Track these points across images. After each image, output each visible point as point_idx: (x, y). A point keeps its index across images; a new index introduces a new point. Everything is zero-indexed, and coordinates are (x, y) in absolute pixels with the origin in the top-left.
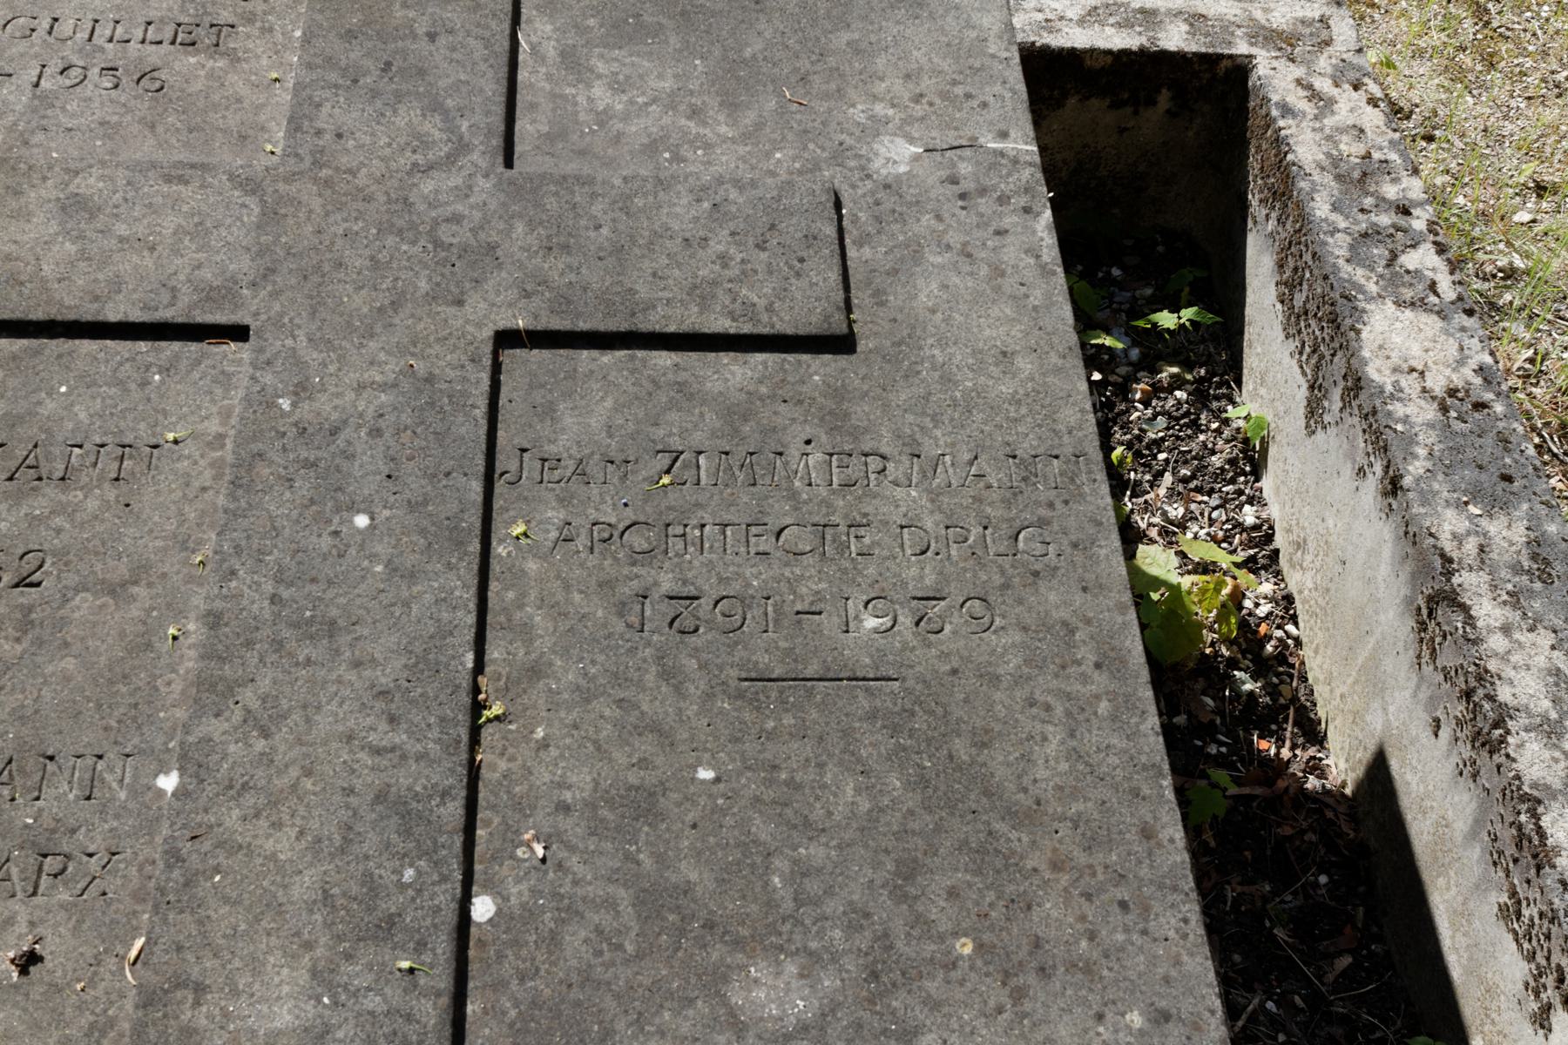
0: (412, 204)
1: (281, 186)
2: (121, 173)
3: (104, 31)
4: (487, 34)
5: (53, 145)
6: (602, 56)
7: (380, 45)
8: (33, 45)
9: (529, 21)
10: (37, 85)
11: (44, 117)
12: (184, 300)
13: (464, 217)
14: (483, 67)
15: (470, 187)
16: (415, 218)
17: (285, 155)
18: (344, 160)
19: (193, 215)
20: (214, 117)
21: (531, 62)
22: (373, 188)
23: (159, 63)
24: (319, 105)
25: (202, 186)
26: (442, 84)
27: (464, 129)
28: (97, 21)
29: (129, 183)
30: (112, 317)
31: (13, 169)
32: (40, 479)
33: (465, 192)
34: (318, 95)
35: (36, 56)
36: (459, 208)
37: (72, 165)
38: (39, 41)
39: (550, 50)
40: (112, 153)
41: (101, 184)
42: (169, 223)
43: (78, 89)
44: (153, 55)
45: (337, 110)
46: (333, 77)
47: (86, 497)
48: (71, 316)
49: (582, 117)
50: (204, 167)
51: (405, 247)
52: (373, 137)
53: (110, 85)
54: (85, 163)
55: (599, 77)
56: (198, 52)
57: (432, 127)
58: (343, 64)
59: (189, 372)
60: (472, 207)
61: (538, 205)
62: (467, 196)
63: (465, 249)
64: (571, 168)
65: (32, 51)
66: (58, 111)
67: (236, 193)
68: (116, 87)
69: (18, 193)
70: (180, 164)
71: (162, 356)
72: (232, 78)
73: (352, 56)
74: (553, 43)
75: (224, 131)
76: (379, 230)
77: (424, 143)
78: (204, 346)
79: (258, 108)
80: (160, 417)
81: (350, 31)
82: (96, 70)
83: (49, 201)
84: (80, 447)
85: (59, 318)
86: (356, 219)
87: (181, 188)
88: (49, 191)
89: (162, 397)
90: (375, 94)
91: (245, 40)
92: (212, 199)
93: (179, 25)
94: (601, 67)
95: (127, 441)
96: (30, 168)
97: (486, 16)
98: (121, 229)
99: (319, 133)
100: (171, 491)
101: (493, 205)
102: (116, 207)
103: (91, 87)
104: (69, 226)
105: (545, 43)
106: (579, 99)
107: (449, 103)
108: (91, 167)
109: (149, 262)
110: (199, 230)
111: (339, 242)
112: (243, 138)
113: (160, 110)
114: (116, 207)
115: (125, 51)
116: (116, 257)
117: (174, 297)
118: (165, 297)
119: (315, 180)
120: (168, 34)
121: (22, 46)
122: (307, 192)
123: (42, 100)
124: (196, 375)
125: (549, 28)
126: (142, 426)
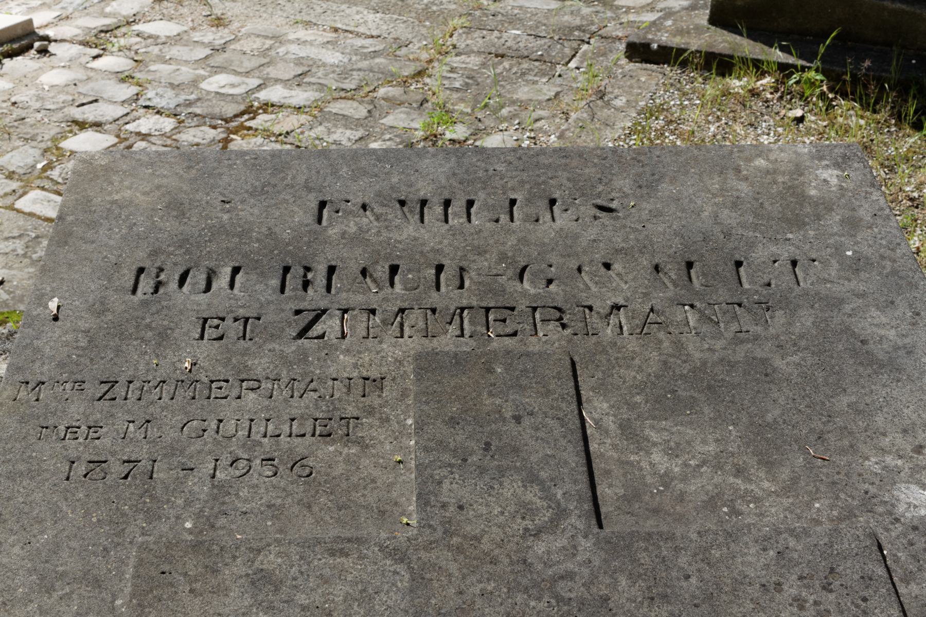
0: (531, 565)
1: (423, 554)
2: (293, 549)
4: (561, 415)
5: (234, 527)
6: (652, 427)
7: (478, 429)
8: (206, 444)
9: (589, 401)
10: (213, 476)
11: (224, 503)
13: (575, 573)
14: (563, 442)
15: (575, 547)
16: (535, 576)
17: (420, 527)
18: (469, 528)
19: (357, 584)
21: (597, 435)
22: (497, 552)
23: (306, 452)
24: (440, 483)
25: (359, 558)
26: (534, 458)
27: (559, 496)
28: (252, 420)
29: (302, 558)
31: (208, 550)
33: (572, 551)
34: (438, 473)
36: (570, 566)
37: (255, 545)
38: (210, 440)
39: (610, 423)
40: (281, 531)
41: (279, 560)
42: (339, 591)
43: (246, 478)
45: (455, 486)
46: (446, 457)
49: (649, 480)
50: (359, 541)
51: (533, 603)
52: (493, 508)
54: (264, 542)
55: (655, 444)
56: (334, 442)
57: (532, 495)
58: (452, 445)
60: (580, 565)
61: (634, 561)
62: (574, 555)
63: (582, 603)
64: (649, 525)
67: (388, 562)
68: (275, 474)
73: (458, 438)
74: (611, 418)
76: (509, 589)
77: (526, 510)
79: (390, 486)
81: (452, 418)
82: (258, 461)
83: (241, 577)
86: (488, 580)
87: (343, 559)
88: (239, 568)
90: (482, 470)
91: (369, 429)
92: (369, 569)
93: (316, 420)
94: (654, 436)
97: (557, 399)
98: (302, 599)
99: (444, 506)
101: (597, 562)
102: (295, 579)
103: (256, 476)
104: (260, 598)
105: (605, 418)
106: (643, 464)
107: (543, 475)
108: (269, 545)
111: (479, 602)
112: (382, 513)
113: (313, 492)
114: (295, 579)
119: (449, 547)
120: (309, 429)
121: (198, 445)
122: (443, 557)
123: (220, 490)
125: (605, 405)
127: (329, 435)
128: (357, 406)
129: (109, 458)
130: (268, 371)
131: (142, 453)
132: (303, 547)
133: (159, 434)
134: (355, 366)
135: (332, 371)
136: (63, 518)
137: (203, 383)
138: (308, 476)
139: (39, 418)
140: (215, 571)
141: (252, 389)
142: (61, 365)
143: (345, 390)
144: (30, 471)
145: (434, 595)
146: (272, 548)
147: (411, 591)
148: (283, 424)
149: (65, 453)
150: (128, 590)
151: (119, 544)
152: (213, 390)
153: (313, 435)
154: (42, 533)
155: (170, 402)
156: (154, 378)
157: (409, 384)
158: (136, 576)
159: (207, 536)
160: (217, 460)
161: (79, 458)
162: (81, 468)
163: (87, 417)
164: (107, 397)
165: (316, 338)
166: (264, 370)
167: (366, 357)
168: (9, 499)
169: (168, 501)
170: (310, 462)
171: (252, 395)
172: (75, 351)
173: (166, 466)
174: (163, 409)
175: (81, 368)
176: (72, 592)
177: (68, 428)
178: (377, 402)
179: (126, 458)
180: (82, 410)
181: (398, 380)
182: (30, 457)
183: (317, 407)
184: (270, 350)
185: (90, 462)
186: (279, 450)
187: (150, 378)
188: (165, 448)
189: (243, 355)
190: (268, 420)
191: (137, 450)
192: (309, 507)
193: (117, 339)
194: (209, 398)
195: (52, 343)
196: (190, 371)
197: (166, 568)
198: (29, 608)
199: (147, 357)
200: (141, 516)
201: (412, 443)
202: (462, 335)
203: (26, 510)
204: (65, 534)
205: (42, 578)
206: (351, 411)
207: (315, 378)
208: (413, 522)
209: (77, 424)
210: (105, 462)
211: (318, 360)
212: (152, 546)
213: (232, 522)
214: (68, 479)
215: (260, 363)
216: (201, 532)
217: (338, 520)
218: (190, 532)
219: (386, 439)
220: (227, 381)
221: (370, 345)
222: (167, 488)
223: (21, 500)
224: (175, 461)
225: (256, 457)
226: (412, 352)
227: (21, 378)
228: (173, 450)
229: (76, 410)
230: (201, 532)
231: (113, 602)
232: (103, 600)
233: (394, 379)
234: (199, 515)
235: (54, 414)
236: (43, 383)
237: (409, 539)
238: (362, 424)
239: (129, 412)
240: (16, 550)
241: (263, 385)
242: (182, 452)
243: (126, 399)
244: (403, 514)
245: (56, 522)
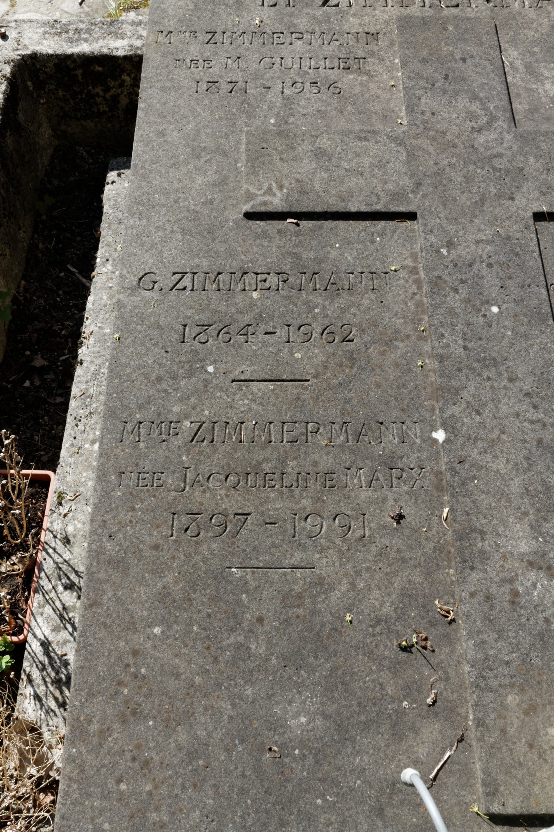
0: (476, 148)
1: (412, 141)
2: (336, 136)
3: (306, 63)
4: (490, 58)
6: (545, 67)
7: (440, 66)
8: (275, 72)
9: (506, 50)
10: (283, 93)
11: (291, 109)
12: (384, 201)
13: (503, 154)
14: (493, 75)
15: (502, 139)
16: (479, 155)
18: (438, 126)
20: (369, 106)
21: (511, 72)
22: (456, 140)
23: (336, 79)
24: (419, 99)
26: (475, 85)
27: (491, 108)
28: (301, 58)
29: (342, 142)
32: (338, 290)
33: (500, 141)
34: (418, 93)
36: (500, 150)
37: (314, 133)
38: (278, 70)
39: (519, 64)
41: (329, 142)
42: (366, 161)
43: (302, 93)
45: (428, 101)
46: (422, 83)
47: (362, 298)
48: (334, 209)
49: (544, 100)
50: (374, 132)
51: (479, 171)
52: (453, 114)
53: (316, 91)
54: (319, 132)
55: (547, 78)
56: (352, 73)
57: (475, 107)
58: (425, 76)
59: (392, 236)
60: (505, 149)
61: (537, 147)
62: (502, 144)
63: (508, 171)
64: (544, 127)
65: (276, 75)
67: (393, 145)
69: (293, 148)
70: (362, 131)
72: (372, 86)
73: (428, 71)
74: (520, 61)
76: (465, 162)
77: (472, 117)
78: (395, 223)
79: (389, 100)
80: (385, 259)
81: (424, 59)
82: (308, 84)
83: (308, 152)
84: (353, 273)
85: (329, 210)
86: (452, 157)
87: (366, 143)
89: (383, 249)
90: (444, 92)
91: (372, 65)
92: (382, 149)
93: (340, 59)
94: (546, 73)
95: (373, 271)
97: (487, 48)
98: (345, 165)
99: (423, 113)
100: (399, 295)
101: (515, 148)
102: (340, 154)
103: (308, 93)
104: (321, 164)
105: (516, 61)
106: (540, 90)
107: (481, 95)
109: (362, 181)
110: (382, 164)
111: (448, 170)
112: (385, 117)
113: (343, 103)
114: (340, 154)
116: (347, 179)
117: (378, 199)
118: (375, 199)
119: (428, 137)
120: (336, 65)
121: (270, 73)
122: (424, 143)
123: (288, 101)
124: (396, 238)
125: (516, 53)
126: (378, 263)
127: (349, 68)
128: (363, 50)
129: (219, 80)
130: (307, 27)
131: (239, 77)
132: (342, 135)
133: (246, 66)
134: (360, 25)
135: (346, 27)
136: (198, 115)
137: (268, 34)
138: (339, 93)
139: (173, 54)
140: (293, 148)
141: (299, 39)
142: (180, 21)
143: (355, 40)
144: (174, 87)
145: (421, 165)
146: (324, 135)
147: (408, 162)
148: (321, 61)
149: (193, 76)
150: (244, 157)
151: (233, 131)
152: (275, 39)
153: (339, 68)
154: (188, 123)
155: (250, 46)
156: (238, 30)
157: (394, 37)
158: (248, 150)
159: (285, 127)
160: (283, 83)
161: (202, 80)
162: (205, 86)
163: (202, 54)
164: (211, 42)
165: (334, 6)
166: (305, 26)
167: (366, 19)
168: (165, 103)
169: (258, 107)
170: (339, 85)
171: (299, 43)
172: (187, 12)
173: (254, 86)
174: (247, 50)
175: (193, 23)
176: (211, 159)
177: (191, 61)
178: (376, 48)
179: (229, 80)
180: (198, 49)
181: (387, 35)
182: (172, 78)
183: (340, 51)
184: (306, 14)
185: (208, 82)
186: (320, 77)
187: (236, 30)
188: (251, 74)
189: (291, 16)
190: (311, 58)
191: (235, 75)
192: (342, 112)
193: (211, 5)
194: (273, 44)
195: (172, 7)
196: (259, 26)
197: (265, 145)
198: (189, 167)
199: (232, 17)
200: (244, 115)
201: (400, 74)
202: (424, 6)
203: (176, 110)
204: (202, 125)
205: (193, 150)
206: (360, 54)
207: (336, 32)
208: (405, 122)
209: (197, 58)
210: (217, 82)
211: (337, 20)
212: (254, 133)
213: (298, 120)
214: (197, 92)
215: (301, 22)
216: (280, 125)
217: (360, 120)
218: (274, 125)
219: (383, 71)
220: (283, 33)
221: (368, 11)
222: (256, 99)
223: (172, 104)
224: (259, 82)
225: (306, 81)
226: (395, 17)
227: (158, 29)
228: (256, 76)
229: (195, 50)
230: (280, 125)
231: (236, 164)
232: (230, 163)
233: (385, 34)
234: (277, 116)
235: (182, 52)
236: (172, 32)
237: (404, 132)
238: (368, 62)
239: (226, 51)
240: (175, 133)
241: (305, 36)
242: (262, 77)
243: (223, 43)
244: (398, 117)
245: (195, 118)
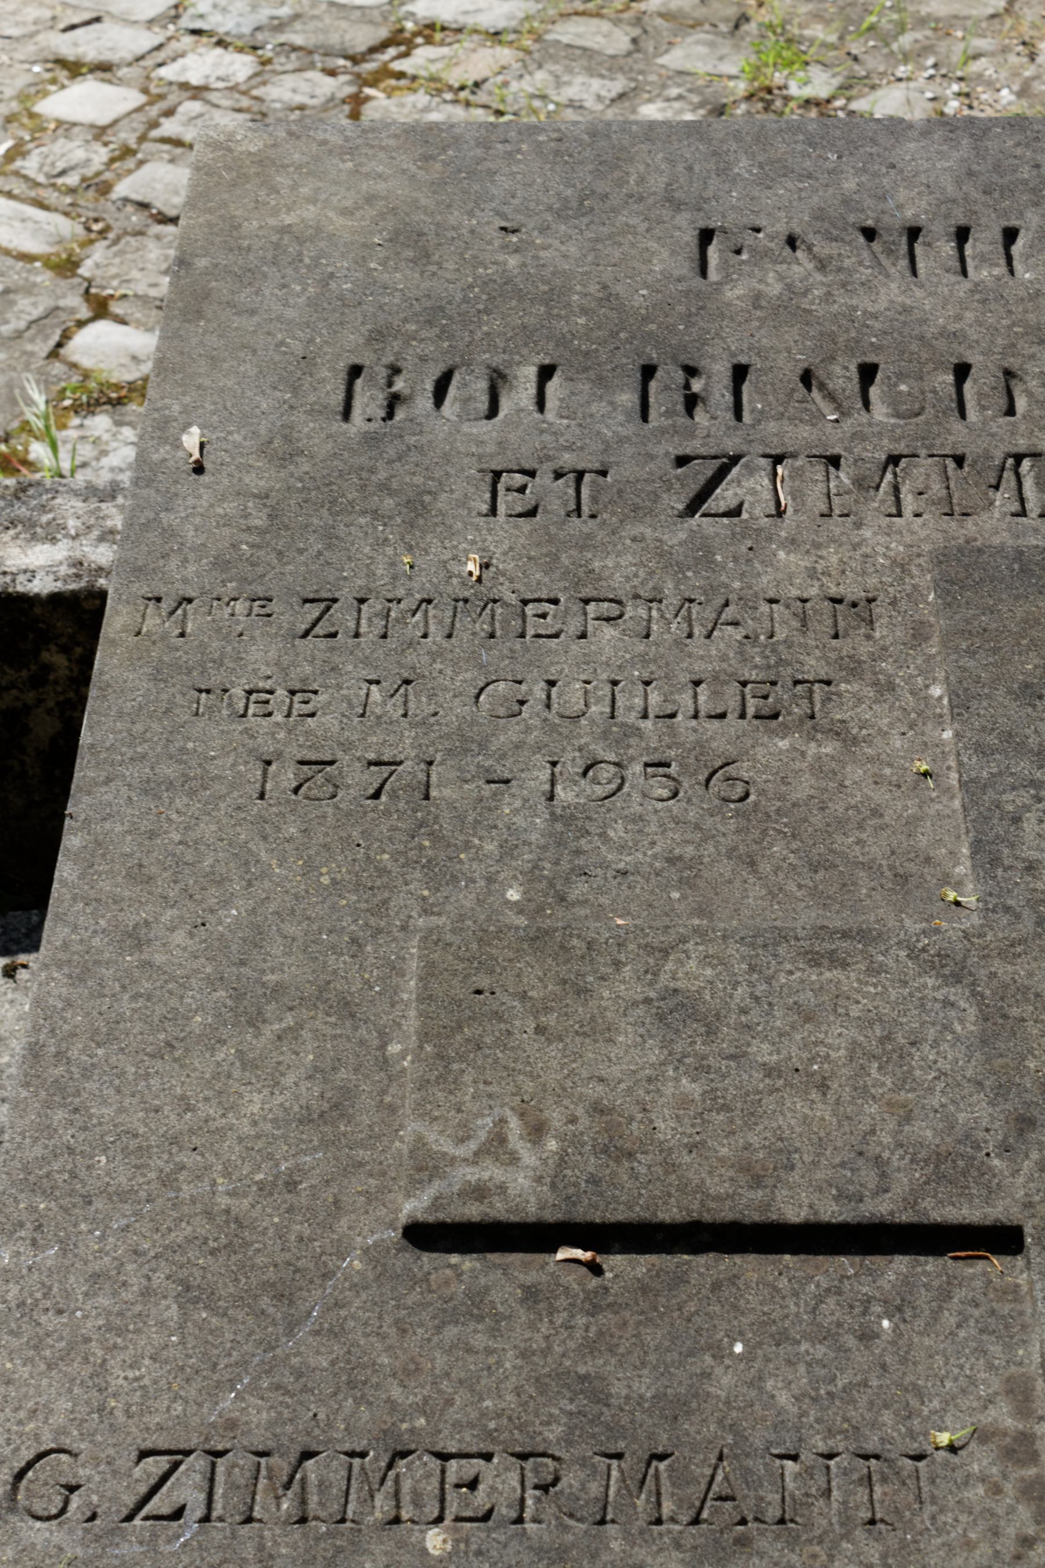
2: (733, 949)
3: (630, 700)
5: (604, 900)
8: (528, 730)
10: (551, 797)
11: (578, 852)
12: (901, 1183)
17: (986, 911)
19: (871, 1024)
20: (844, 842)
23: (732, 751)
24: (1017, 820)
25: (871, 971)
28: (615, 683)
29: (752, 969)
30: (794, 1213)
31: (562, 947)
32: (743, 1522)
35: (538, 748)
37: (656, 939)
38: (535, 722)
40: (700, 912)
41: (709, 972)
42: (838, 1037)
43: (618, 801)
44: (722, 737)
46: (1024, 767)
47: (831, 1558)
48: (726, 1214)
50: (864, 935)
53: (665, 793)
54: (672, 937)
56: (785, 731)
59: (936, 1315)
65: (531, 738)
66: (597, 842)
67: (930, 982)
68: (675, 795)
69: (583, 992)
70: (820, 932)
71: (883, 1283)
72: (854, 773)
75: (868, 867)
78: (945, 1263)
79: (913, 822)
80: (914, 1403)
82: (638, 768)
83: (635, 1004)
84: (794, 1458)
85: (707, 1218)
87: (837, 973)
88: (628, 985)
89: (904, 1361)
91: (853, 704)
92: (893, 994)
93: (744, 684)
95: (870, 1447)
96: (590, 945)
98: (763, 1052)
100: (969, 1545)
102: (744, 1011)
103: (636, 797)
104: (678, 1048)
108: (684, 940)
109: (823, 1111)
110: (892, 1050)
113: (756, 834)
114: (744, 1011)
115: (673, 732)
116: (769, 1103)
117: (883, 1175)
118: (869, 1177)
120: (732, 704)
121: (510, 733)
123: (568, 823)
124: (949, 1319)
126: (887, 1417)
127: (775, 716)
128: (824, 657)
129: (340, 755)
130: (636, 582)
131: (405, 745)
132: (752, 945)
133: (432, 708)
134: (812, 573)
135: (765, 582)
136: (263, 875)
137: (507, 605)
138: (742, 799)
139: (189, 672)
140: (583, 992)
141: (608, 619)
142: (221, 564)
143: (796, 624)
144: (186, 778)
145: (1031, 1051)
146: (690, 946)
147: (984, 1042)
148: (680, 691)
149: (251, 743)
150: (412, 1023)
151: (379, 931)
152: (530, 620)
153: (743, 716)
154: (226, 904)
155: (445, 644)
156: (409, 593)
157: (925, 612)
158: (425, 997)
159: (556, 918)
160: (554, 764)
161: (280, 755)
162: (286, 776)
163: (285, 671)
164: (318, 630)
165: (725, 515)
166: (628, 579)
167: (832, 557)
168: (152, 835)
169: (467, 845)
170: (743, 770)
171: (609, 632)
172: (244, 536)
173: (454, 774)
174: (435, 656)
175: (260, 570)
176: (300, 1025)
177: (250, 692)
178: (865, 649)
179: (372, 756)
180: (272, 654)
181: (903, 605)
182: (183, 750)
183: (744, 658)
184: (634, 539)
185: (302, 763)
186: (678, 745)
187: (400, 592)
188: (448, 736)
189: (583, 548)
190: (647, 683)
191: (391, 738)
192: (752, 864)
193: (324, 512)
194: (522, 635)
195: (198, 520)
196: (479, 580)
197: (484, 981)
198: (220, 1056)
199: (389, 551)
200: (417, 874)
201: (948, 735)
202: (1023, 513)
203: (189, 857)
204: (272, 907)
205: (238, 996)
206: (813, 666)
207: (733, 597)
208: (970, 900)
209: (268, 685)
210: (331, 763)
211: (735, 560)
212: (449, 937)
213: (600, 891)
214: (262, 796)
215: (618, 566)
216: (540, 910)
217: (814, 892)
218: (519, 908)
219: (891, 725)
220: (555, 602)
221: (837, 531)
222: (461, 819)
223: (177, 837)
224: (472, 763)
225: (632, 759)
226: (926, 547)
227: (145, 591)
228: (465, 743)
229: (262, 657)
230: (540, 910)
231: (383, 1047)
232: (362, 1043)
233: (894, 603)
234: (531, 875)
235: (219, 663)
236: (190, 601)
237: (966, 935)
238: (839, 695)
239: (366, 661)
240: (179, 937)
241: (629, 612)
242: (483, 746)
243: (357, 635)
244: (946, 880)
245: (250, 884)
